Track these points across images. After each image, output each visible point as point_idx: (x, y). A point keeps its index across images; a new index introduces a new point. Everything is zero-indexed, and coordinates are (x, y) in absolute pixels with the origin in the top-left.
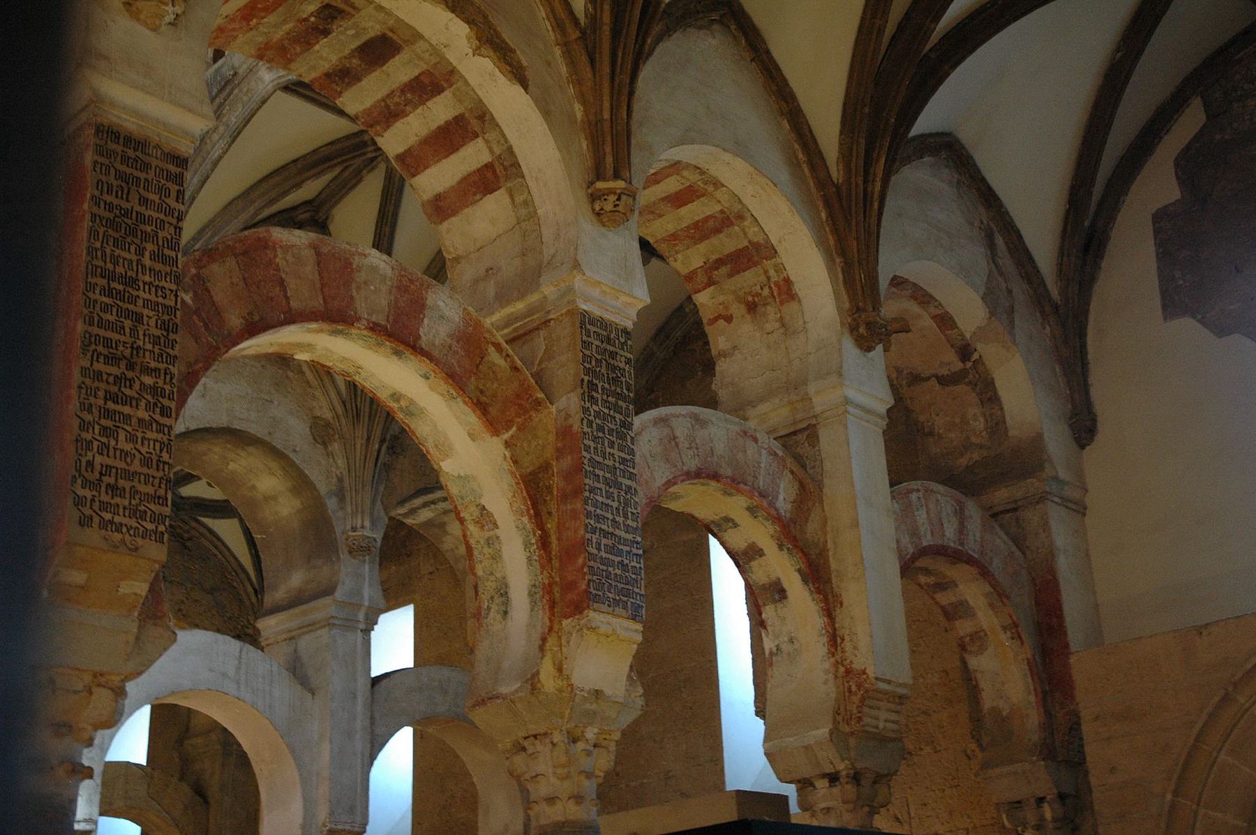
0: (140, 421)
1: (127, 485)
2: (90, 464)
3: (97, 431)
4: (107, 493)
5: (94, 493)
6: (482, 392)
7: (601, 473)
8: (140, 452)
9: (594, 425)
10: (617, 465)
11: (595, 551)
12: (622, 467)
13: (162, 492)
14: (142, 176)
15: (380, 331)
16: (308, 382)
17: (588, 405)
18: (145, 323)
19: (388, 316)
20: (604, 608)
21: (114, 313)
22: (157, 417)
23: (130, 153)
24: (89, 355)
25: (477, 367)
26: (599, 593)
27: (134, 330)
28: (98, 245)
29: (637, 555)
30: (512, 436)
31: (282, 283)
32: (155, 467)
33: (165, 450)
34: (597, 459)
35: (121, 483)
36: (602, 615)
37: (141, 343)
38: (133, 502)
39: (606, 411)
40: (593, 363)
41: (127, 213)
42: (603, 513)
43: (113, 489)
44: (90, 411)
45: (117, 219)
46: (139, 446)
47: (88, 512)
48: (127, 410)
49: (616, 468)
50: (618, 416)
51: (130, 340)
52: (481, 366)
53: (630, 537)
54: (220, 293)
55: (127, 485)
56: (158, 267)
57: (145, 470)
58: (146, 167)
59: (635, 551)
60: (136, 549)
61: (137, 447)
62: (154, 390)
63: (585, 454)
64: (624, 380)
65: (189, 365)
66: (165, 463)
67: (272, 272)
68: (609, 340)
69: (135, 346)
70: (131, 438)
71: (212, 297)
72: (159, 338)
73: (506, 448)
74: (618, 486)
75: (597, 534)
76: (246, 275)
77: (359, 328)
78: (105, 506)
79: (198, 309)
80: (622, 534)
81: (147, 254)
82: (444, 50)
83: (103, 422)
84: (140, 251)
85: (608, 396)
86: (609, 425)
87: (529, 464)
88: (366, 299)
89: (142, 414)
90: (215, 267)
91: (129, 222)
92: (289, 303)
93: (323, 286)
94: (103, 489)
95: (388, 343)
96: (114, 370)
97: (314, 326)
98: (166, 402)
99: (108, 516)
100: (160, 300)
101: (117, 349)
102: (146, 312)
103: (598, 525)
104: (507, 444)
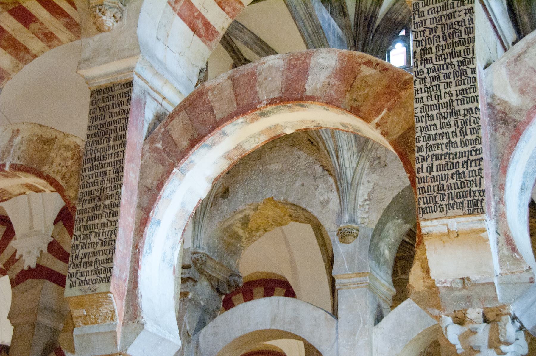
0: (103, 225)
1: (93, 259)
2: (77, 256)
3: (82, 238)
4: (84, 267)
5: (78, 269)
6: (355, 100)
7: (435, 112)
8: (101, 240)
9: (428, 80)
10: (454, 98)
11: (425, 174)
12: (460, 97)
13: (110, 256)
14: (110, 103)
15: (276, 102)
17: (420, 67)
18: (108, 174)
19: (281, 91)
20: (438, 214)
21: (94, 177)
22: (111, 219)
24: (81, 203)
25: (352, 85)
26: (430, 205)
28: (89, 148)
29: (476, 160)
30: (382, 117)
31: (211, 110)
32: (107, 244)
33: (113, 234)
34: (431, 103)
35: (91, 259)
37: (105, 186)
38: (96, 267)
39: (443, 62)
40: (427, 33)
41: (102, 125)
43: (87, 264)
44: (80, 230)
45: (99, 131)
46: (101, 237)
47: (74, 279)
48: (96, 222)
49: (453, 101)
50: (455, 61)
51: (99, 187)
52: (354, 84)
53: (469, 148)
54: (176, 135)
55: (93, 259)
57: (103, 248)
58: (113, 97)
59: (472, 158)
60: (95, 290)
61: (100, 238)
62: (111, 206)
63: (416, 105)
64: (462, 29)
65: (159, 179)
66: (112, 240)
67: (206, 106)
69: (102, 188)
70: (97, 235)
71: (172, 138)
72: (114, 178)
73: (377, 128)
74: (455, 113)
75: (429, 160)
76: (191, 116)
77: (264, 108)
78: (82, 274)
79: (165, 148)
80: (459, 149)
81: (112, 140)
83: (85, 233)
84: (109, 141)
85: (443, 50)
86: (446, 71)
87: (397, 132)
88: (266, 87)
89: (104, 220)
90: (174, 122)
91: (104, 129)
92: (215, 118)
94: (82, 265)
95: (289, 105)
96: (92, 205)
98: (115, 209)
99: (83, 278)
100: (116, 159)
101: (94, 194)
102: (109, 168)
103: (430, 154)
104: (378, 125)
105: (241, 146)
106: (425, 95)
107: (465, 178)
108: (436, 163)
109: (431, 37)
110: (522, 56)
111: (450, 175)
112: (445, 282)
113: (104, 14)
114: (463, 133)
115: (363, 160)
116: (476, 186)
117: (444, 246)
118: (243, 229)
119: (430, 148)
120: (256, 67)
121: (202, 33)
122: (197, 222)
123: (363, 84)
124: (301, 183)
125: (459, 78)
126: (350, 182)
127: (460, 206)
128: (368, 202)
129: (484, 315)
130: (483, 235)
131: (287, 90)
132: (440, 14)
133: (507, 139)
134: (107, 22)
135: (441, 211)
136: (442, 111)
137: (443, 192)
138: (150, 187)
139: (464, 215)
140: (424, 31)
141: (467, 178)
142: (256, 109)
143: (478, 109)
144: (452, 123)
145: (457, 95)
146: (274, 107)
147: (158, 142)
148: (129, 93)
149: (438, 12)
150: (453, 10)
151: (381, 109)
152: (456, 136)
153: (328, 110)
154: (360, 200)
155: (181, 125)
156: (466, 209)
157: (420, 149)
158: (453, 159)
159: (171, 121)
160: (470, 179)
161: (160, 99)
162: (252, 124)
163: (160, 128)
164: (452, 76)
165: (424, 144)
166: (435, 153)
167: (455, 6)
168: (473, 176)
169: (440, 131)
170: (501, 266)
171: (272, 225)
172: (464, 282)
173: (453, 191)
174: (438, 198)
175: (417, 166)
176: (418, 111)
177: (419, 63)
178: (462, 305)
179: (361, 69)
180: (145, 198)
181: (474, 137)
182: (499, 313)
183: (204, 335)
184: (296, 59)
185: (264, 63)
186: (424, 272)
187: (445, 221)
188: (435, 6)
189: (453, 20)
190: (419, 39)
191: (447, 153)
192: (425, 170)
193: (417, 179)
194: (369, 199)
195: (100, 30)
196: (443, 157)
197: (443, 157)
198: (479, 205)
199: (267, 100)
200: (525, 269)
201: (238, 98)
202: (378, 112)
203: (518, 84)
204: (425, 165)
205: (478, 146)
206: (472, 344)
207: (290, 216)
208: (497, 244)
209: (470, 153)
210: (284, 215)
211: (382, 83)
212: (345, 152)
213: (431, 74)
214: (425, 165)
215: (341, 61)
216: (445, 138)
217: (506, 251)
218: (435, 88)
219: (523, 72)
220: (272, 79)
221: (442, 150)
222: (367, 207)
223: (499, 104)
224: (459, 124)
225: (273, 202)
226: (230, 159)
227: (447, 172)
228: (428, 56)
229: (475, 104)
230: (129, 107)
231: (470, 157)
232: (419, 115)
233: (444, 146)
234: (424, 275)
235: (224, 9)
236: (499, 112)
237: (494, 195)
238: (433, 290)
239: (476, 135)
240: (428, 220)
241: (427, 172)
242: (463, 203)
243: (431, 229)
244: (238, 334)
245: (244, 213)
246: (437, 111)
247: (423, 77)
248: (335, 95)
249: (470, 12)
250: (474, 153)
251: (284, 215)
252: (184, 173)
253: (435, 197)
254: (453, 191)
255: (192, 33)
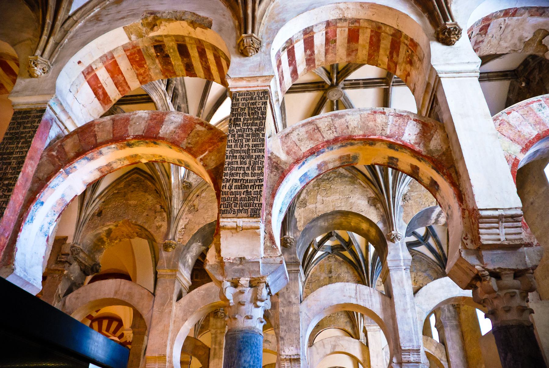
6: (189, 143)
7: (238, 155)
9: (236, 136)
10: (250, 148)
11: (227, 190)
12: (254, 148)
14: (26, 120)
16: (364, 187)
22: (6, 193)
23: (24, 115)
25: (189, 134)
26: (227, 209)
27: (6, 169)
29: (259, 185)
30: (205, 156)
31: (95, 136)
34: (236, 149)
36: (229, 219)
37: (7, 171)
40: (239, 110)
41: (17, 133)
42: (238, 172)
49: (249, 150)
50: (253, 128)
51: (3, 171)
53: (256, 178)
56: (23, 145)
58: (30, 117)
59: (256, 184)
63: (227, 149)
64: (260, 112)
65: (49, 174)
66: (3, 208)
68: (252, 99)
71: (64, 150)
74: (250, 157)
75: (231, 182)
76: (81, 138)
80: (250, 178)
81: (21, 143)
82: (190, 35)
84: (18, 143)
85: (247, 121)
86: (247, 133)
87: (212, 165)
88: (134, 128)
90: (68, 140)
93: (113, 131)
95: (147, 141)
97: (113, 146)
98: (11, 187)
102: (14, 161)
103: (232, 178)
105: (111, 165)
106: (233, 144)
107: (251, 195)
108: (234, 184)
109: (242, 112)
110: (290, 135)
111: (242, 192)
112: (230, 259)
113: (36, 66)
114: (253, 169)
115: (184, 206)
116: (257, 200)
117: (232, 236)
118: (107, 237)
119: (232, 175)
120: (130, 116)
121: (101, 98)
122: (78, 228)
123: (196, 135)
124: (146, 214)
125: (255, 138)
126: (175, 216)
127: (246, 211)
128: (184, 230)
129: (250, 282)
130: (257, 231)
131: (147, 131)
132: (248, 101)
133: (277, 178)
134: (37, 72)
135: (233, 213)
136: (242, 154)
137: (236, 202)
138: (41, 178)
139: (248, 217)
140: (237, 109)
141: (253, 195)
142: (125, 140)
143: (264, 157)
144: (248, 162)
145: (252, 147)
146: (137, 141)
147: (54, 151)
148: (41, 116)
149: (247, 100)
150: (255, 101)
151: (205, 151)
152: (249, 170)
153: (171, 148)
154: (179, 228)
155: (72, 143)
156: (250, 213)
157: (226, 175)
158: (245, 183)
159: (66, 140)
160: (254, 196)
161: (63, 128)
162: (120, 151)
163: (58, 143)
164: (251, 136)
165: (229, 172)
166: (235, 178)
167: (257, 99)
168: (256, 194)
169: (240, 166)
170: (264, 253)
171: (125, 237)
172: (241, 260)
173: (243, 202)
174: (233, 205)
175: (223, 184)
176: (228, 152)
177: (232, 126)
178: (238, 275)
179: (196, 127)
180: (36, 185)
181: (260, 172)
182: (259, 281)
183: (70, 298)
184: (157, 115)
185: (136, 114)
186: (216, 252)
187: (235, 220)
188: (246, 97)
189: (255, 106)
190: (234, 112)
191: (242, 179)
192: (227, 188)
193: (221, 193)
194: (185, 228)
195: (31, 76)
196: (239, 181)
197: (239, 181)
198: (258, 212)
199: (133, 136)
200: (278, 255)
201: (115, 132)
202: (203, 152)
203: (286, 149)
204: (228, 184)
205: (261, 178)
206: (240, 300)
207: (137, 233)
208: (264, 239)
209: (256, 181)
210: (133, 233)
211: (208, 136)
212: (175, 199)
213: (239, 133)
214: (228, 184)
215: (184, 120)
216: (242, 170)
217: (268, 244)
218: (240, 141)
219: (289, 143)
220: (139, 124)
221: (240, 177)
222: (183, 232)
223: (274, 158)
224: (252, 163)
225: (128, 223)
226: (102, 172)
227: (240, 190)
228: (238, 123)
229: (263, 153)
230: (39, 124)
231: (256, 183)
232: (228, 155)
233: (241, 175)
234: (216, 254)
235: (118, 88)
236: (274, 162)
237: (266, 209)
238: (221, 263)
239: (261, 171)
240: (225, 218)
241: (229, 188)
242: (248, 210)
243: (226, 223)
244: (92, 299)
245: (109, 227)
246: (239, 154)
247: (234, 133)
248: (177, 139)
249: (264, 104)
250: (258, 181)
251: (133, 233)
252: (68, 173)
253: (231, 204)
254: (243, 202)
255: (94, 96)
